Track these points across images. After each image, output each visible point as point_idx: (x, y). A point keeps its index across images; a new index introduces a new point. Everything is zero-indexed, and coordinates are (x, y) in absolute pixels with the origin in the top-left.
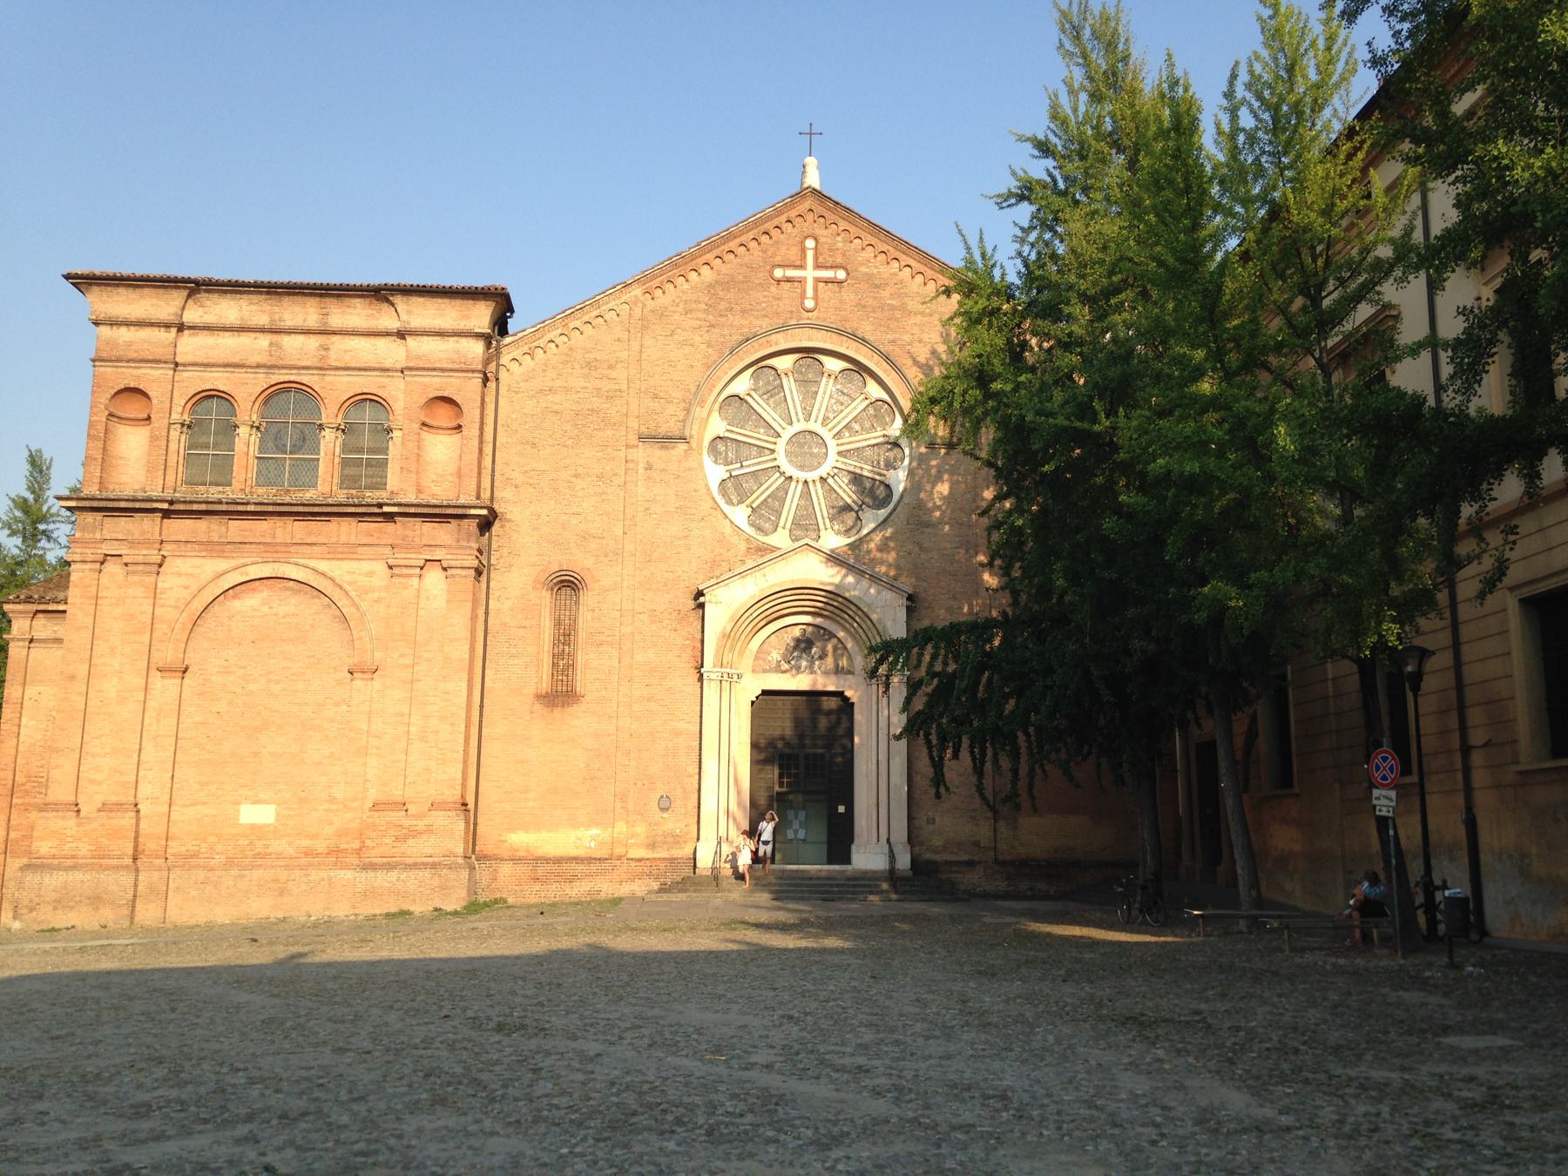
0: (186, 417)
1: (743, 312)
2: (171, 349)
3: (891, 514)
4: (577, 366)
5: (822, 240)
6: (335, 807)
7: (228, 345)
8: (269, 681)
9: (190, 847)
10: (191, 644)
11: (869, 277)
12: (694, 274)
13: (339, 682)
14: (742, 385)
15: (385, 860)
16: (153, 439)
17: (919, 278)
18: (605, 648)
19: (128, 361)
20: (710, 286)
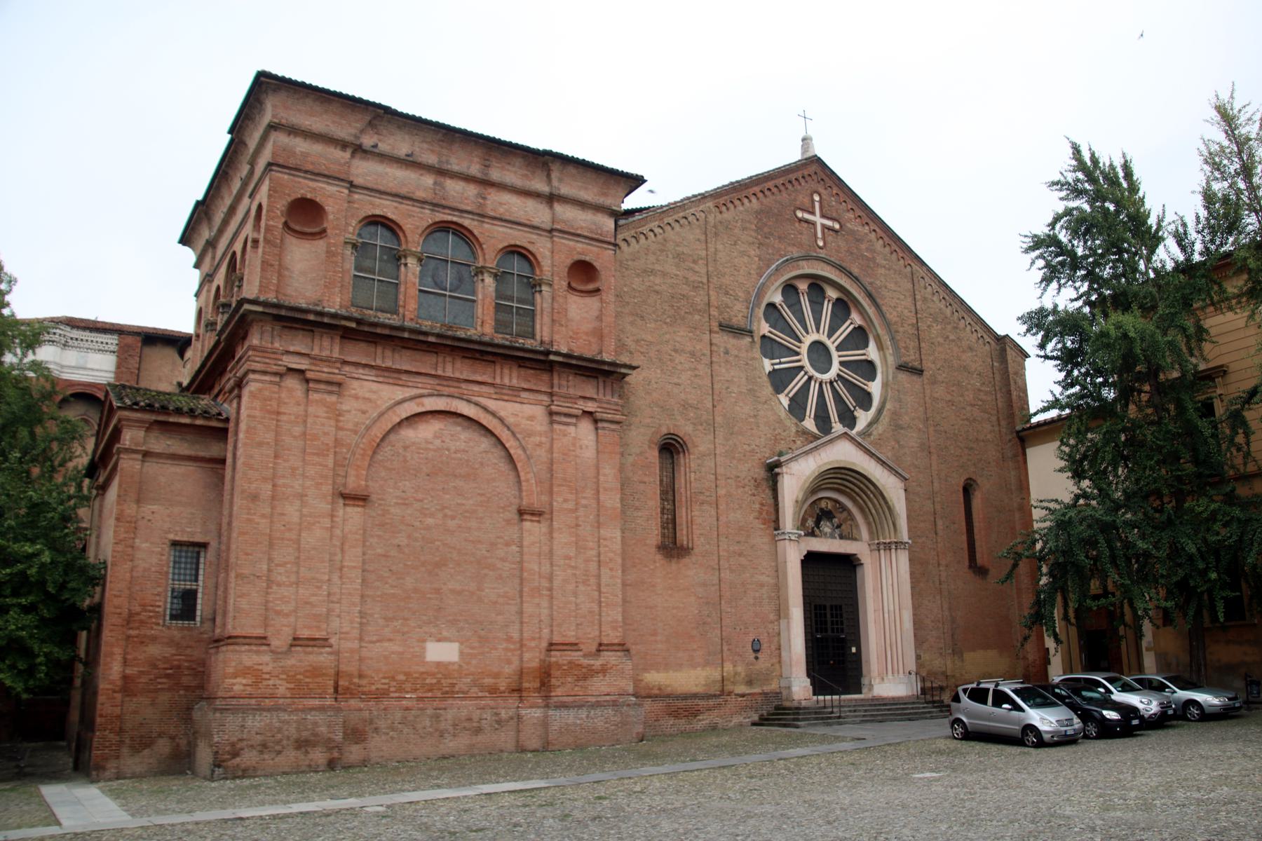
4: (670, 256)
5: (824, 197)
6: (512, 647)
7: (397, 177)
8: (445, 516)
9: (380, 686)
11: (852, 232)
12: (746, 201)
13: (508, 522)
14: (778, 299)
15: (571, 699)
16: (330, 254)
17: (881, 242)
18: (706, 507)
19: (306, 172)
20: (758, 213)
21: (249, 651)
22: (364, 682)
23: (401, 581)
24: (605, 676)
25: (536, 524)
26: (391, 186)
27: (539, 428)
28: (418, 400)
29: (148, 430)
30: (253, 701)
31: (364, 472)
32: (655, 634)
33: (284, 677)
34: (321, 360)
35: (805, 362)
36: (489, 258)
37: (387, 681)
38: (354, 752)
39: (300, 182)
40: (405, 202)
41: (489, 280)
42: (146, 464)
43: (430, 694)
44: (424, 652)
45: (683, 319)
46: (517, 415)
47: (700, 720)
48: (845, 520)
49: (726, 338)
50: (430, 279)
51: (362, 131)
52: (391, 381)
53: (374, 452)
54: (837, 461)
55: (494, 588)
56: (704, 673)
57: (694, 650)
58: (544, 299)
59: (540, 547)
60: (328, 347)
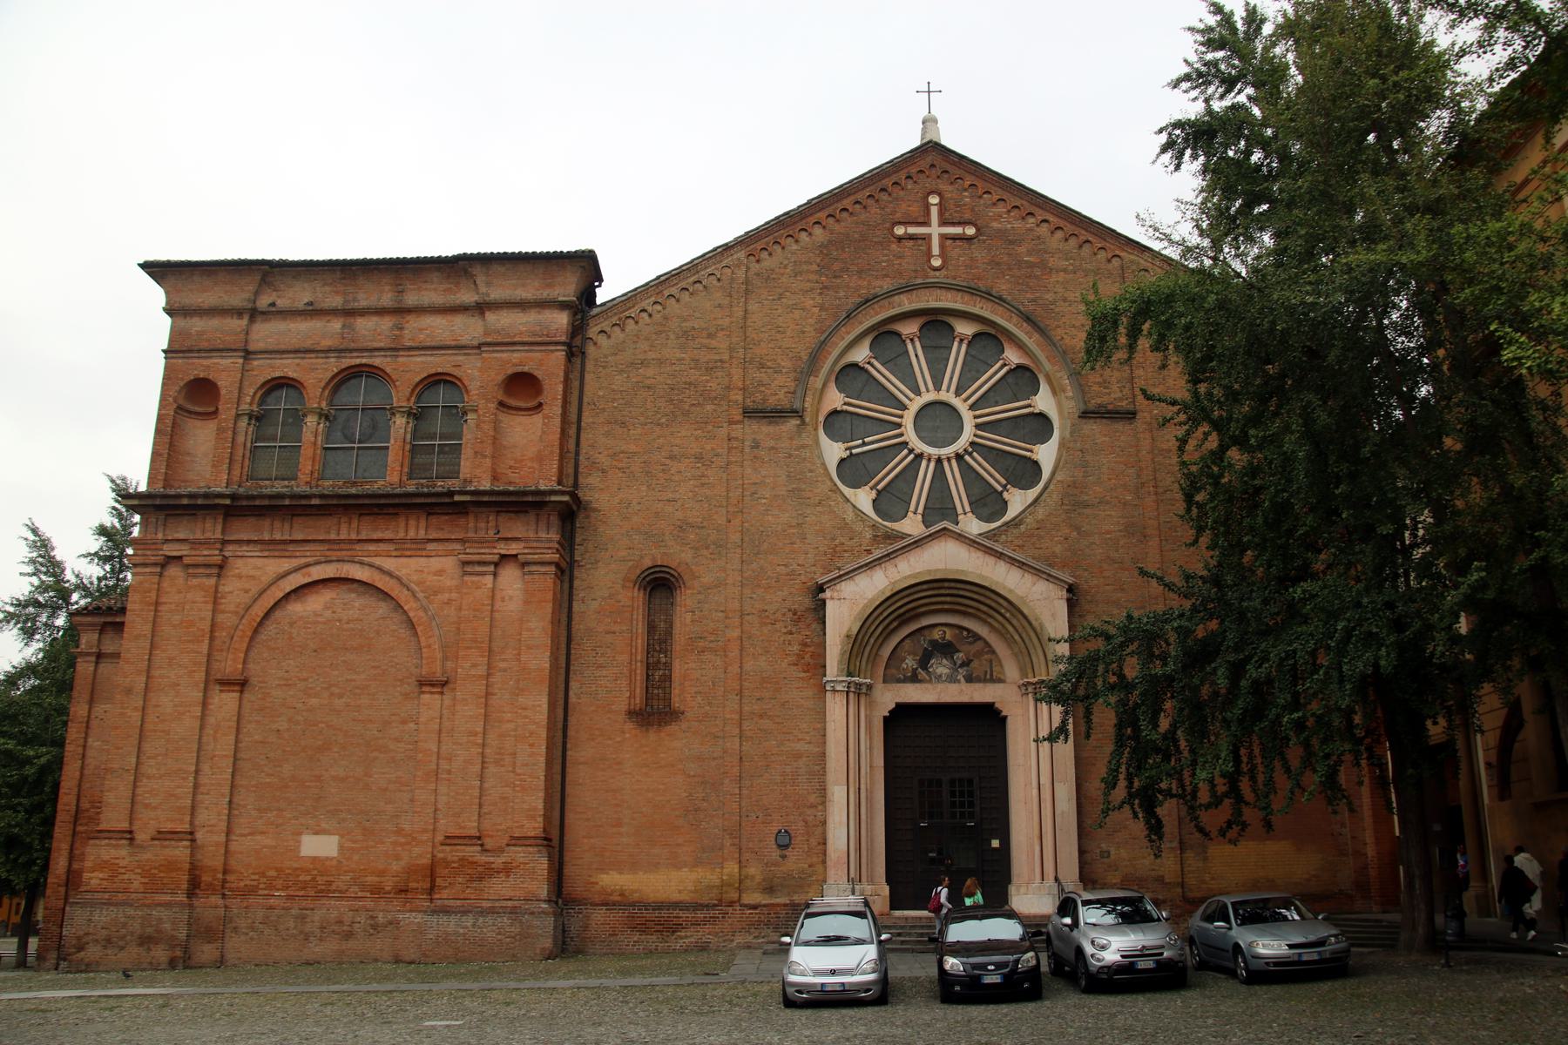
0: (255, 408)
1: (860, 272)
2: (242, 336)
3: (1041, 494)
4: (672, 337)
8: (332, 694)
9: (248, 882)
10: (252, 654)
11: (1001, 234)
13: (406, 696)
14: (861, 354)
16: (220, 430)
17: (1059, 234)
18: (707, 656)
19: (199, 351)
20: (823, 248)
21: (108, 845)
22: (228, 877)
23: (278, 769)
24: (508, 876)
25: (437, 696)
26: (295, 343)
27: (448, 583)
28: (304, 570)
29: (102, 632)
30: (106, 896)
31: (242, 655)
32: (619, 824)
33: (139, 871)
34: (200, 543)
35: (910, 435)
36: (401, 396)
37: (256, 877)
38: (207, 952)
39: (194, 363)
40: (307, 356)
41: (400, 421)
42: (101, 666)
43: (302, 893)
44: (299, 846)
45: (686, 414)
46: (422, 571)
47: (681, 938)
48: (979, 654)
49: (755, 427)
50: (339, 434)
51: (257, 293)
52: (277, 554)
53: (256, 631)
54: (929, 572)
55: (384, 773)
56: (693, 876)
57: (678, 845)
58: (471, 431)
59: (440, 723)
60: (212, 529)
